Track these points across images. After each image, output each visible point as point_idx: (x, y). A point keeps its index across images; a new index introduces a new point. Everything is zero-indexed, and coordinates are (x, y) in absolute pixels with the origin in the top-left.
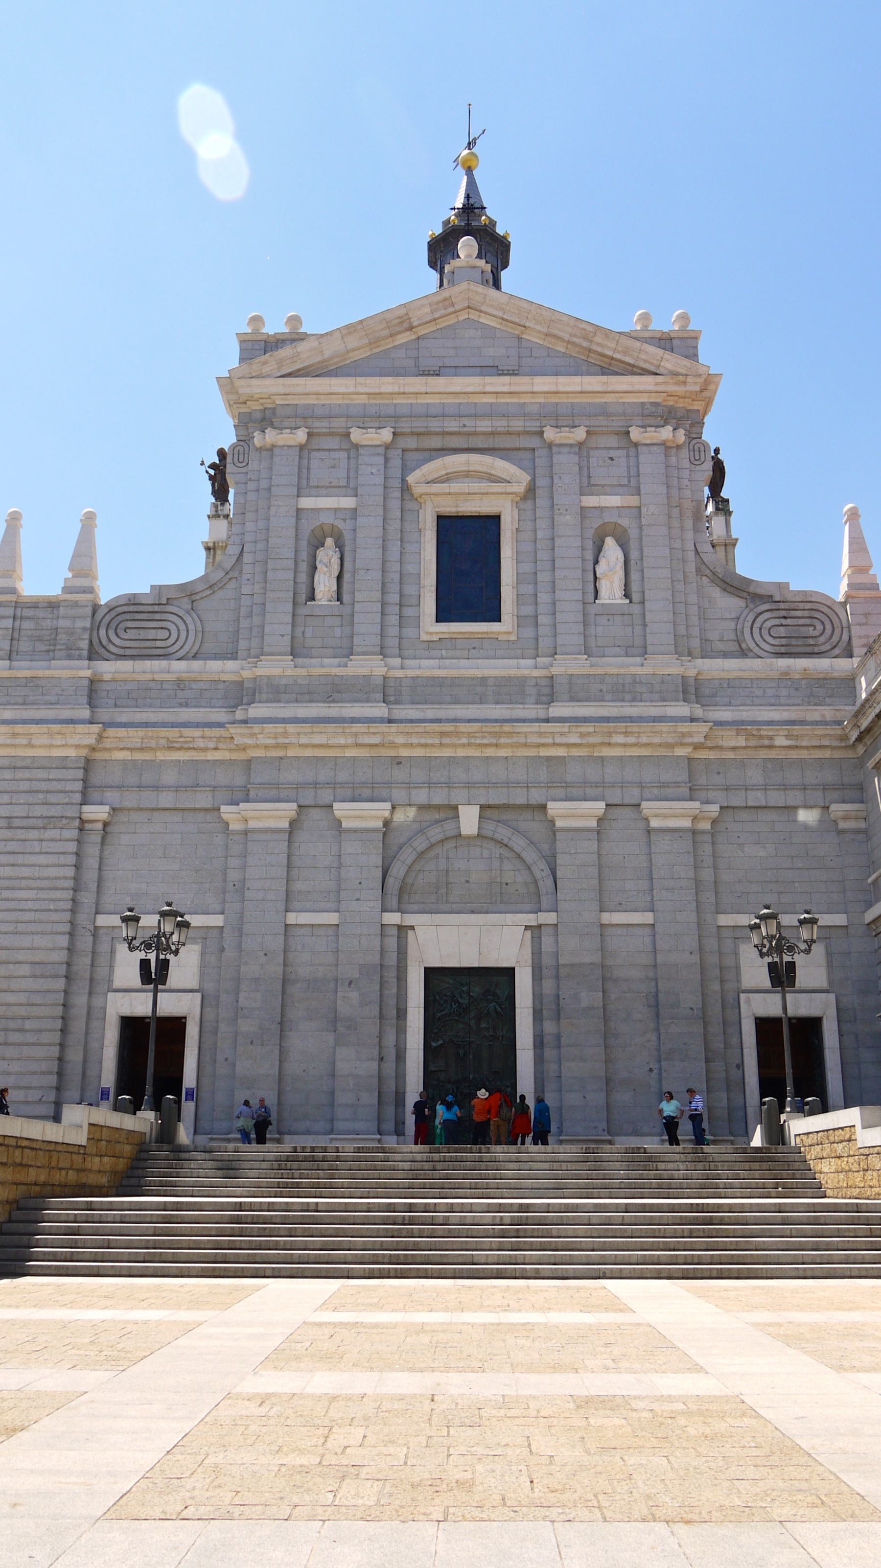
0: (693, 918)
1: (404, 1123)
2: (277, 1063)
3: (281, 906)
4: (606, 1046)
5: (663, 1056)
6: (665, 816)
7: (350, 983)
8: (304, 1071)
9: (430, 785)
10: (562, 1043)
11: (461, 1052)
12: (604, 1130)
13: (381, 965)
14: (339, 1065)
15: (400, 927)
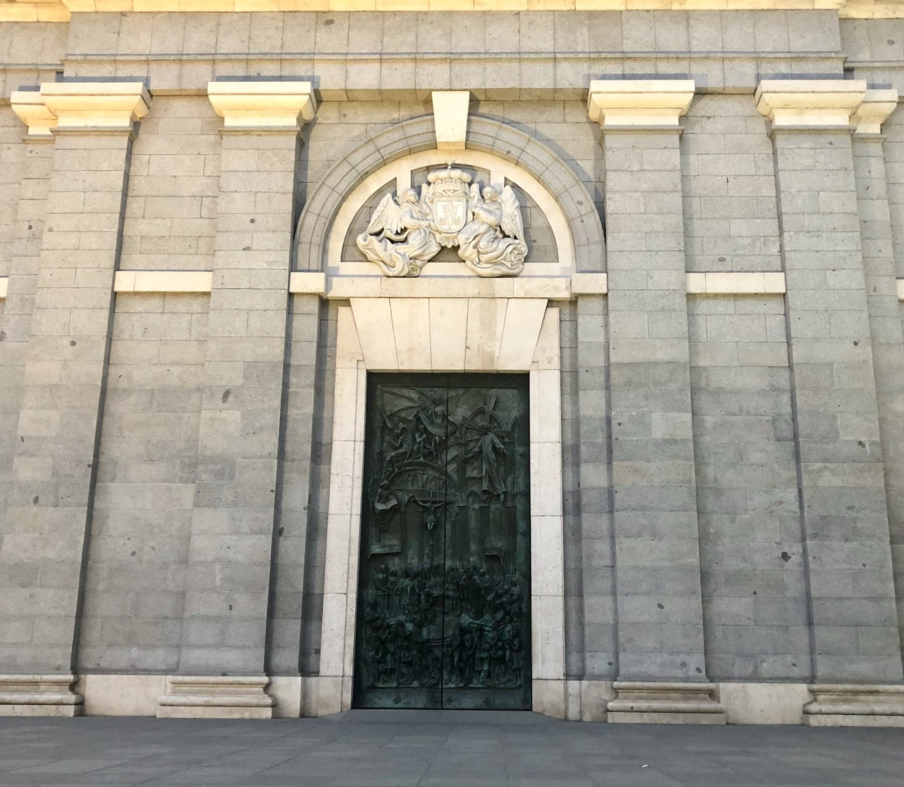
0: (856, 280)
1: (318, 652)
2: (82, 539)
3: (108, 260)
4: (700, 512)
5: (809, 531)
6: (801, 109)
7: (226, 394)
8: (134, 553)
9: (382, 58)
10: (617, 504)
11: (430, 520)
12: (699, 670)
13: (287, 366)
14: (199, 543)
15: (324, 303)
